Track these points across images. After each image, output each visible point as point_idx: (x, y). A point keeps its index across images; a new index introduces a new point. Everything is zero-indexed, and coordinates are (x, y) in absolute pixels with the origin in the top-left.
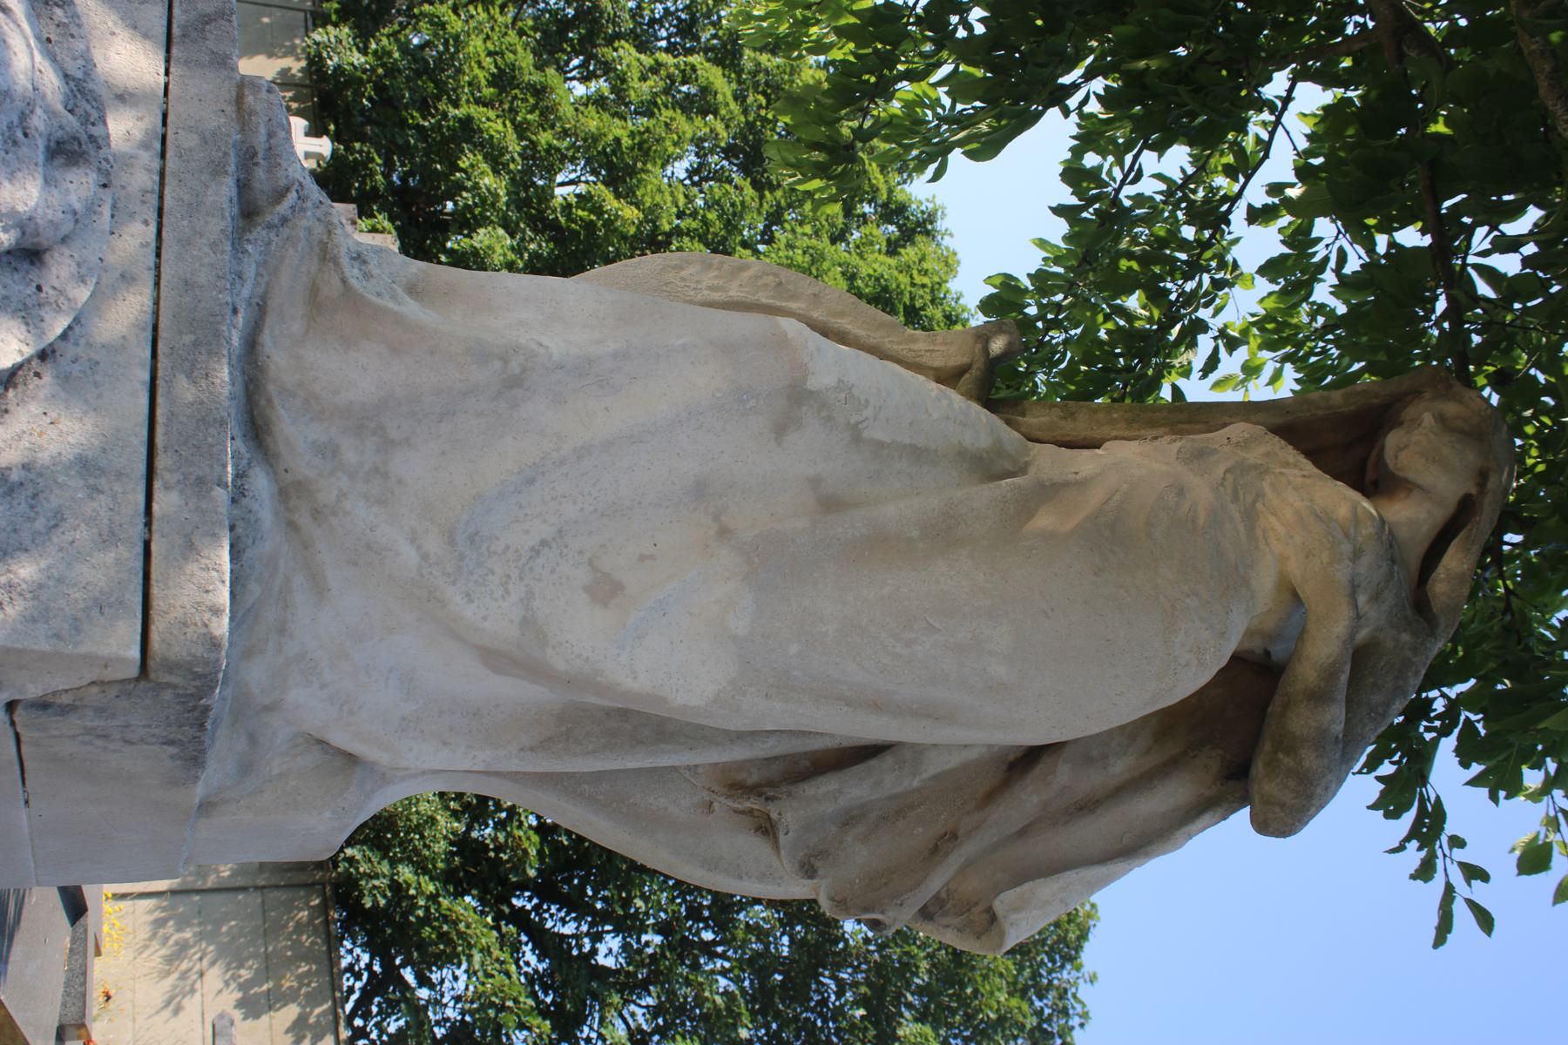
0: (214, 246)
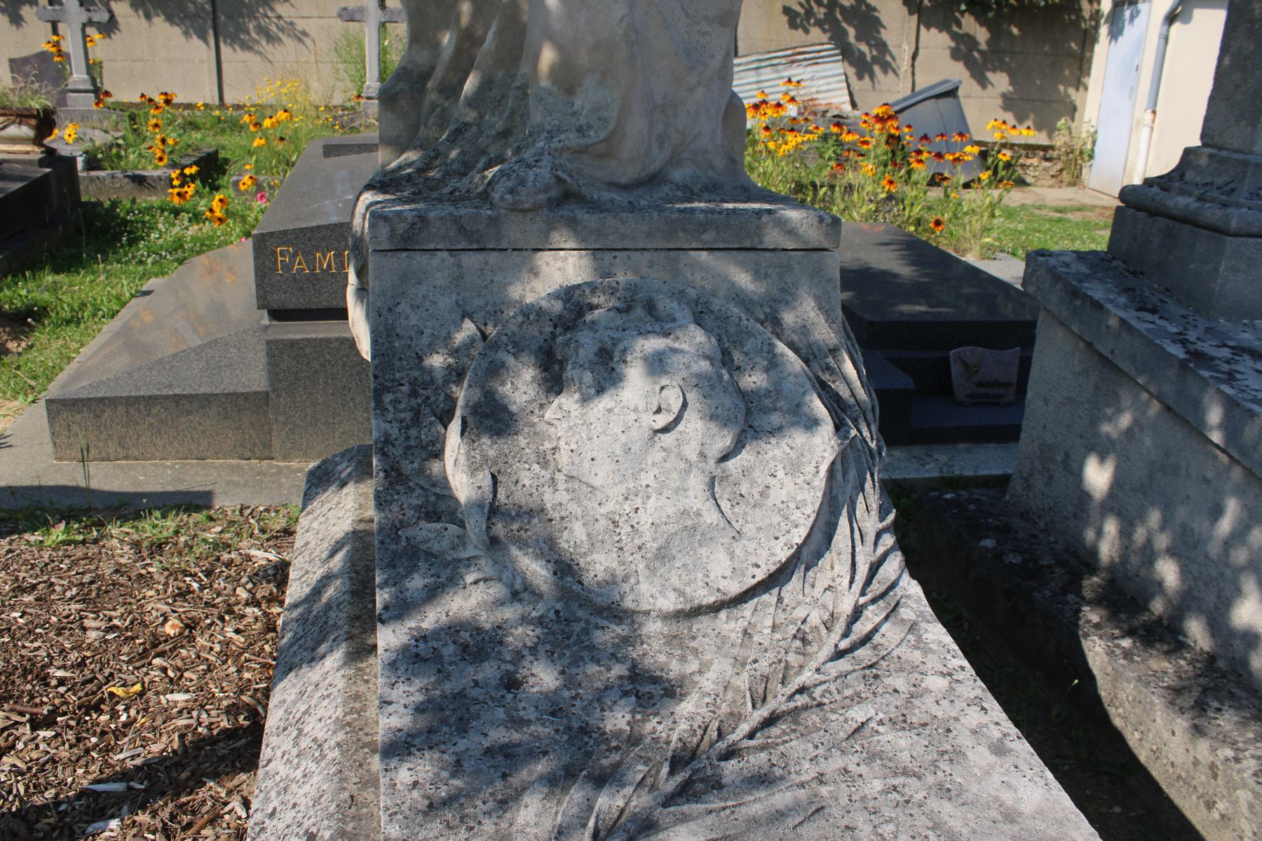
0: (623, 222)
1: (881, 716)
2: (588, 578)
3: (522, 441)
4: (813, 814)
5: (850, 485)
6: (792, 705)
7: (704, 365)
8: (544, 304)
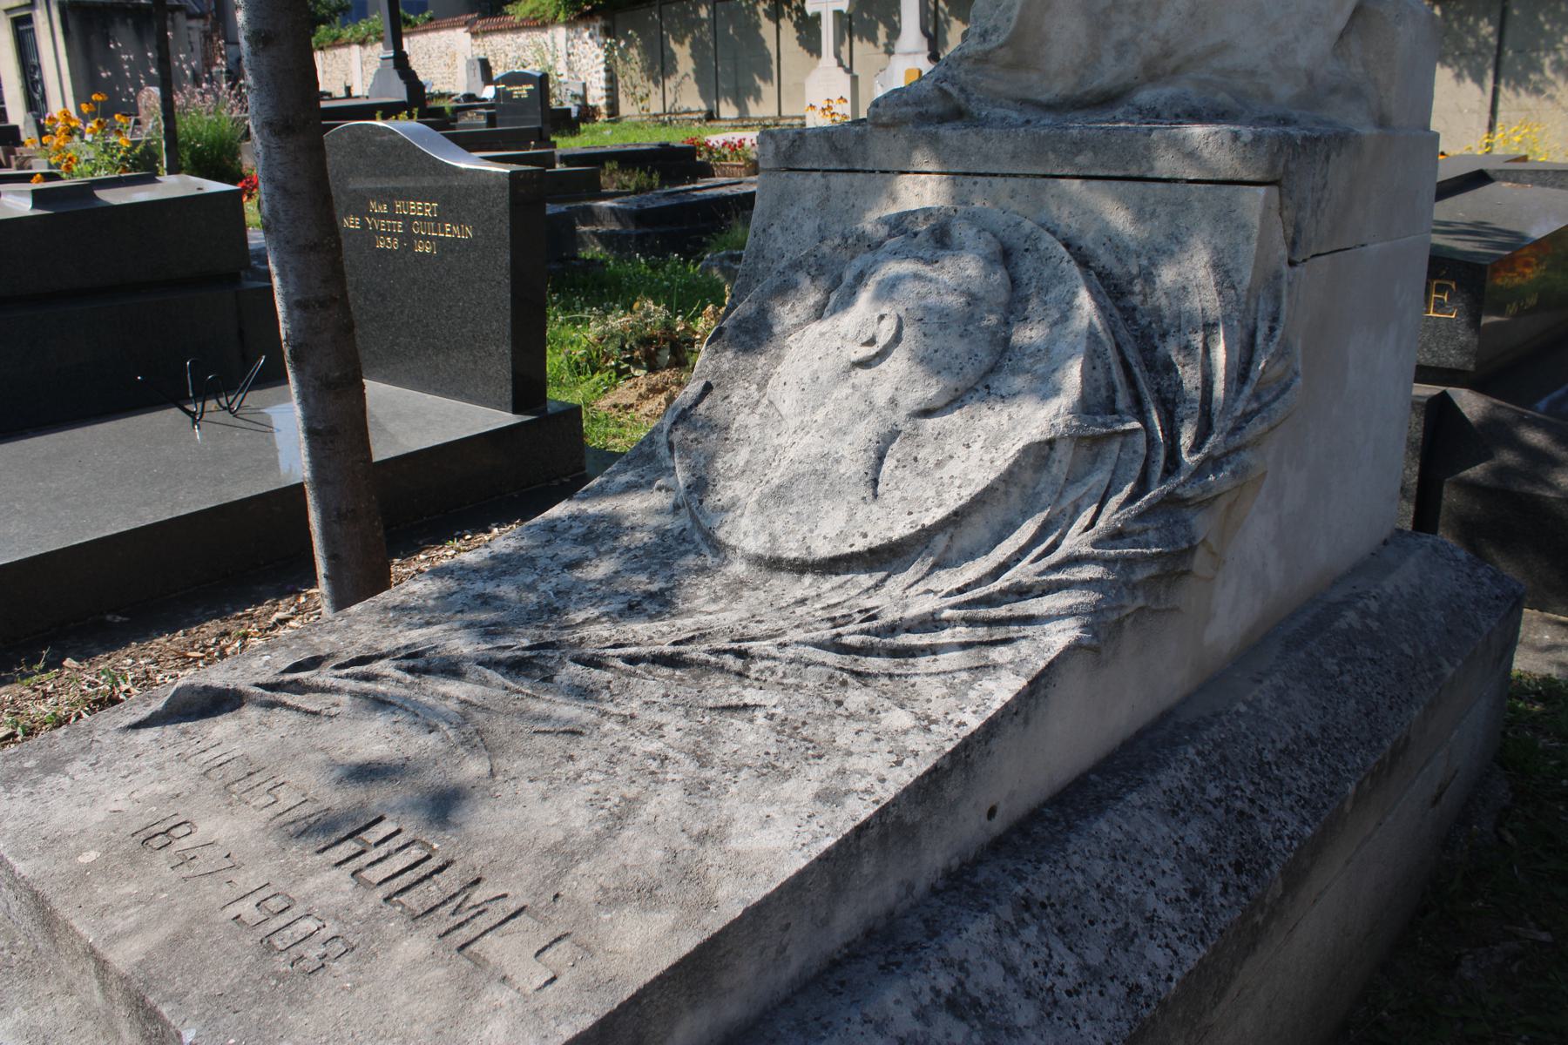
0: (987, 140)
1: (779, 710)
2: (711, 501)
3: (762, 360)
4: (565, 732)
5: (1085, 489)
6: (704, 656)
7: (954, 301)
8: (869, 228)
